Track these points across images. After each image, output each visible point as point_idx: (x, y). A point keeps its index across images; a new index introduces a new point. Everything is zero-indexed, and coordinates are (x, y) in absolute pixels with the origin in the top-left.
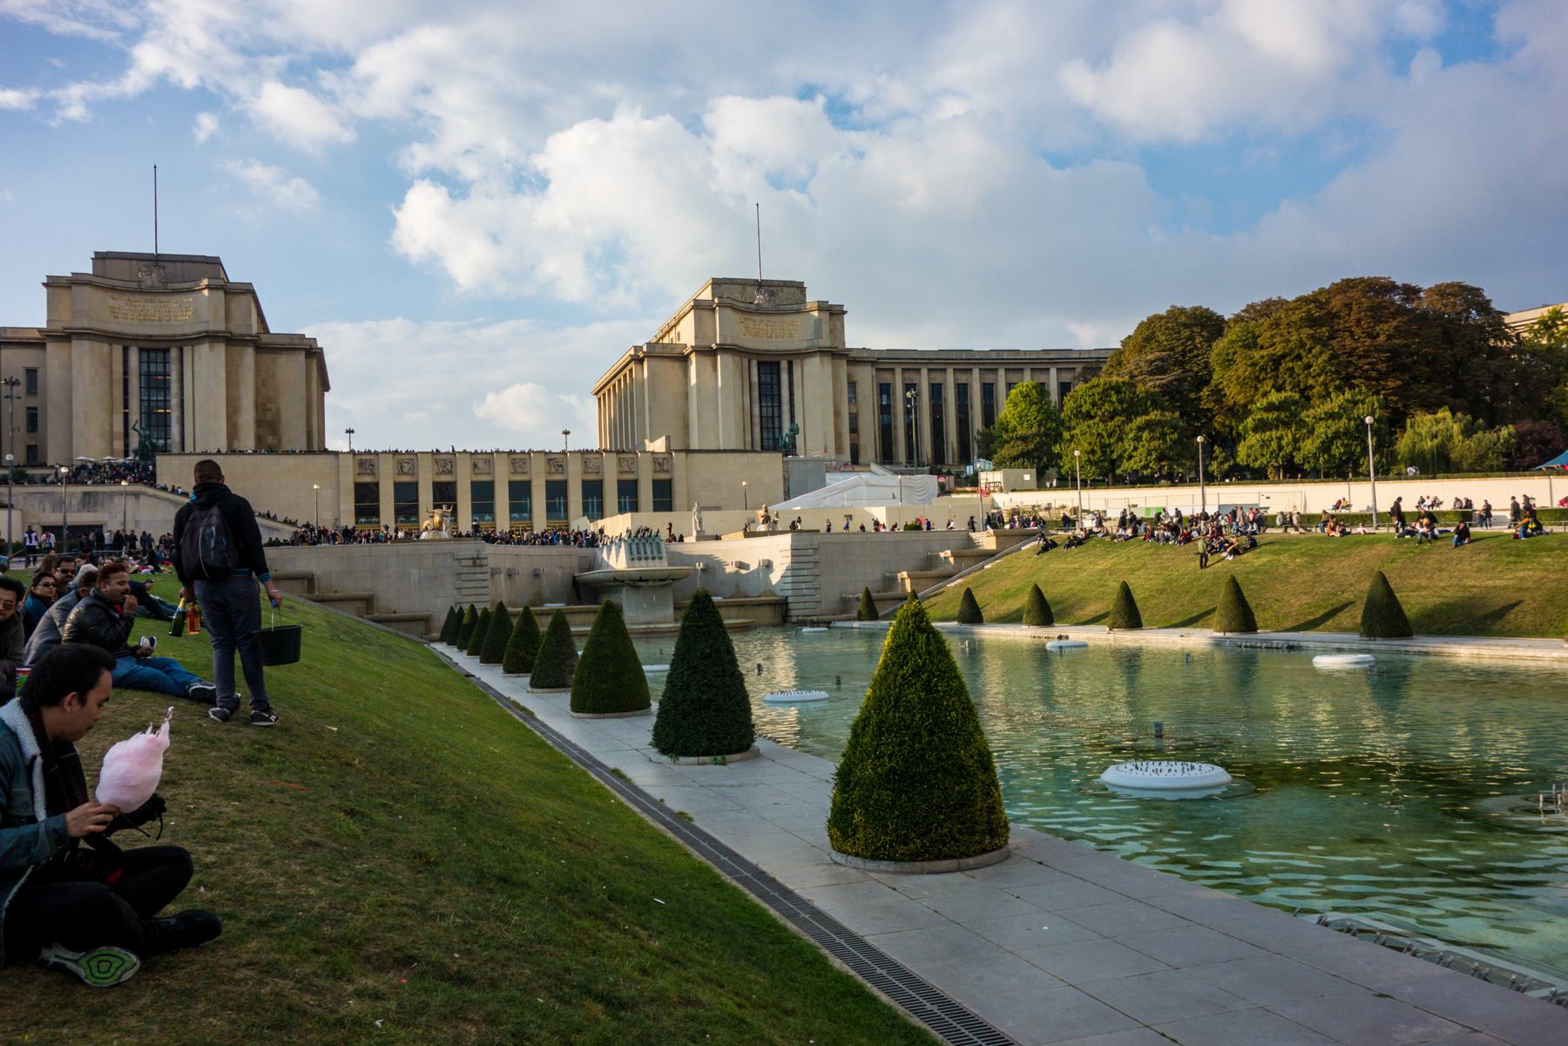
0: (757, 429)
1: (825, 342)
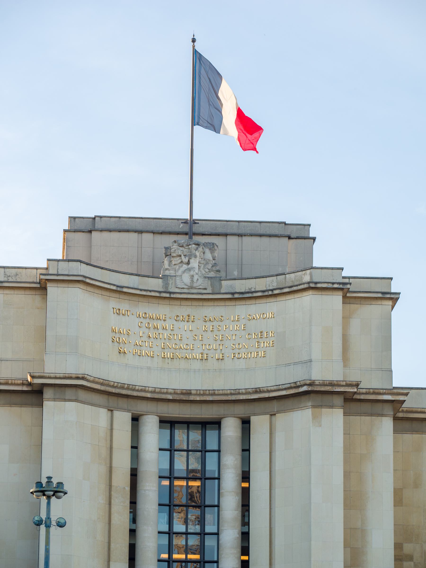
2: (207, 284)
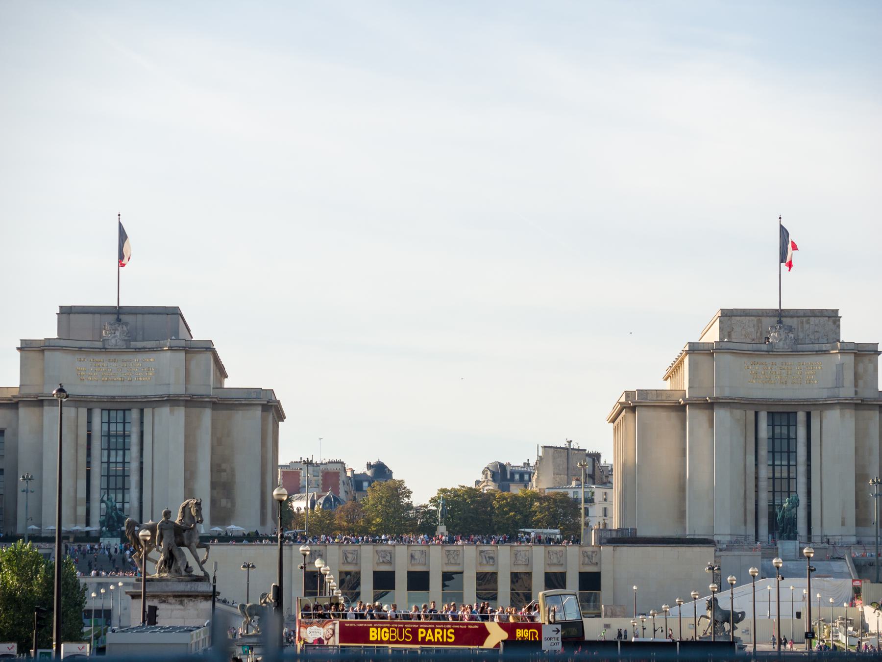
1: (847, 392)
2: (124, 343)
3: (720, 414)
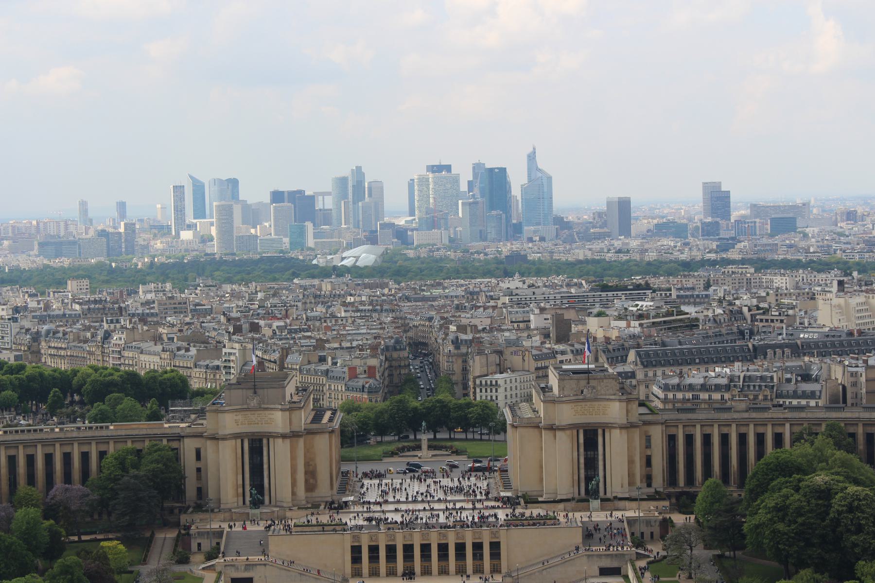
0: (582, 471)
3: (559, 434)
